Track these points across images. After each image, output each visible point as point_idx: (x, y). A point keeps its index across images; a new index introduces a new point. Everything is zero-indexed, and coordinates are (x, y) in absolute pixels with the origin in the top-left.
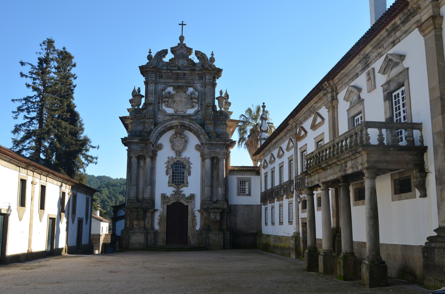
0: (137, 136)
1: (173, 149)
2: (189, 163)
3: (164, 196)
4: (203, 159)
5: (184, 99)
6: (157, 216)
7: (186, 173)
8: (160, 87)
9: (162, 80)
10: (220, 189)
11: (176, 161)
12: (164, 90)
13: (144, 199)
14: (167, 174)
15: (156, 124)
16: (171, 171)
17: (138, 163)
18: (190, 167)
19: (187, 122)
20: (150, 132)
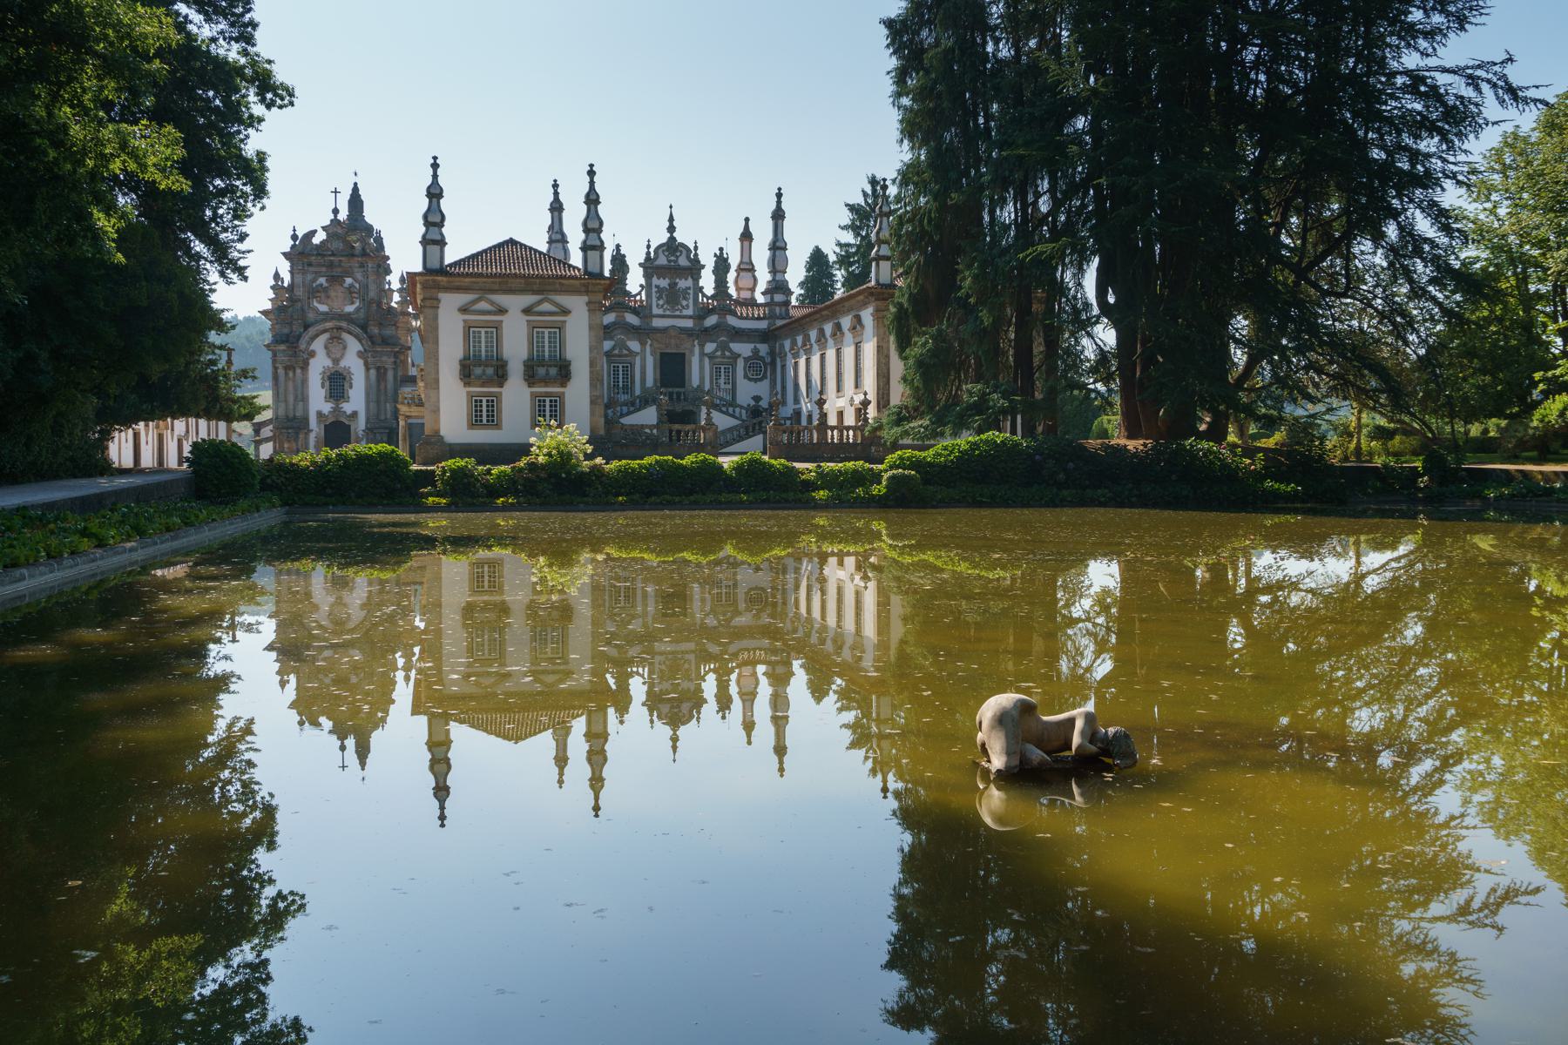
0: (283, 342)
1: (330, 357)
2: (349, 373)
3: (320, 414)
4: (367, 369)
5: (340, 294)
6: (312, 436)
7: (346, 385)
8: (309, 277)
9: (311, 269)
10: (388, 405)
11: (333, 371)
12: (314, 280)
13: (295, 417)
14: (323, 387)
15: (306, 327)
16: (327, 384)
17: (286, 374)
18: (351, 379)
19: (344, 324)
20: (299, 337)
